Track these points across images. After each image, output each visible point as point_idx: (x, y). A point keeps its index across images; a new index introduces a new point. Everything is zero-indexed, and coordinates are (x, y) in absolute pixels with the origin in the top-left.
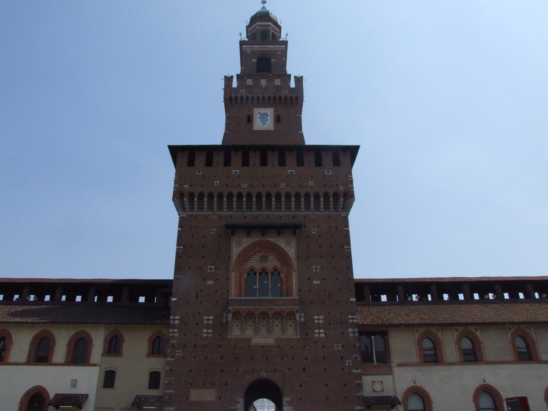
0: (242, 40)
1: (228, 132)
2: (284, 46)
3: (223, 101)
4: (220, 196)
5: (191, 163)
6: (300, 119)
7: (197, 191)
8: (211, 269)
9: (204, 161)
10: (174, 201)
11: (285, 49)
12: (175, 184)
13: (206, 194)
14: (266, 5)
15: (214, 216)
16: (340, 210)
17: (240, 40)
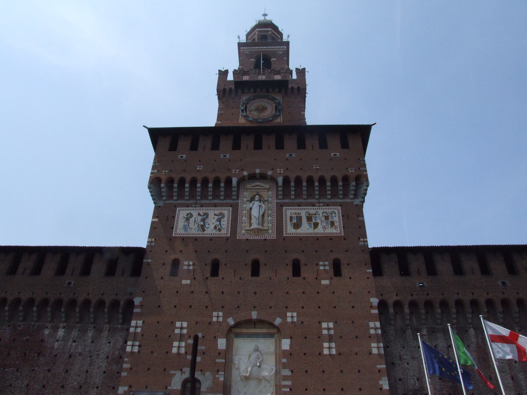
0: (240, 42)
1: (220, 122)
2: (285, 47)
3: (217, 94)
4: (205, 181)
7: (176, 177)
8: (189, 265)
10: (149, 188)
11: (286, 49)
12: (153, 169)
13: (188, 178)
14: (266, 18)
15: (196, 204)
16: (352, 196)
17: (238, 42)
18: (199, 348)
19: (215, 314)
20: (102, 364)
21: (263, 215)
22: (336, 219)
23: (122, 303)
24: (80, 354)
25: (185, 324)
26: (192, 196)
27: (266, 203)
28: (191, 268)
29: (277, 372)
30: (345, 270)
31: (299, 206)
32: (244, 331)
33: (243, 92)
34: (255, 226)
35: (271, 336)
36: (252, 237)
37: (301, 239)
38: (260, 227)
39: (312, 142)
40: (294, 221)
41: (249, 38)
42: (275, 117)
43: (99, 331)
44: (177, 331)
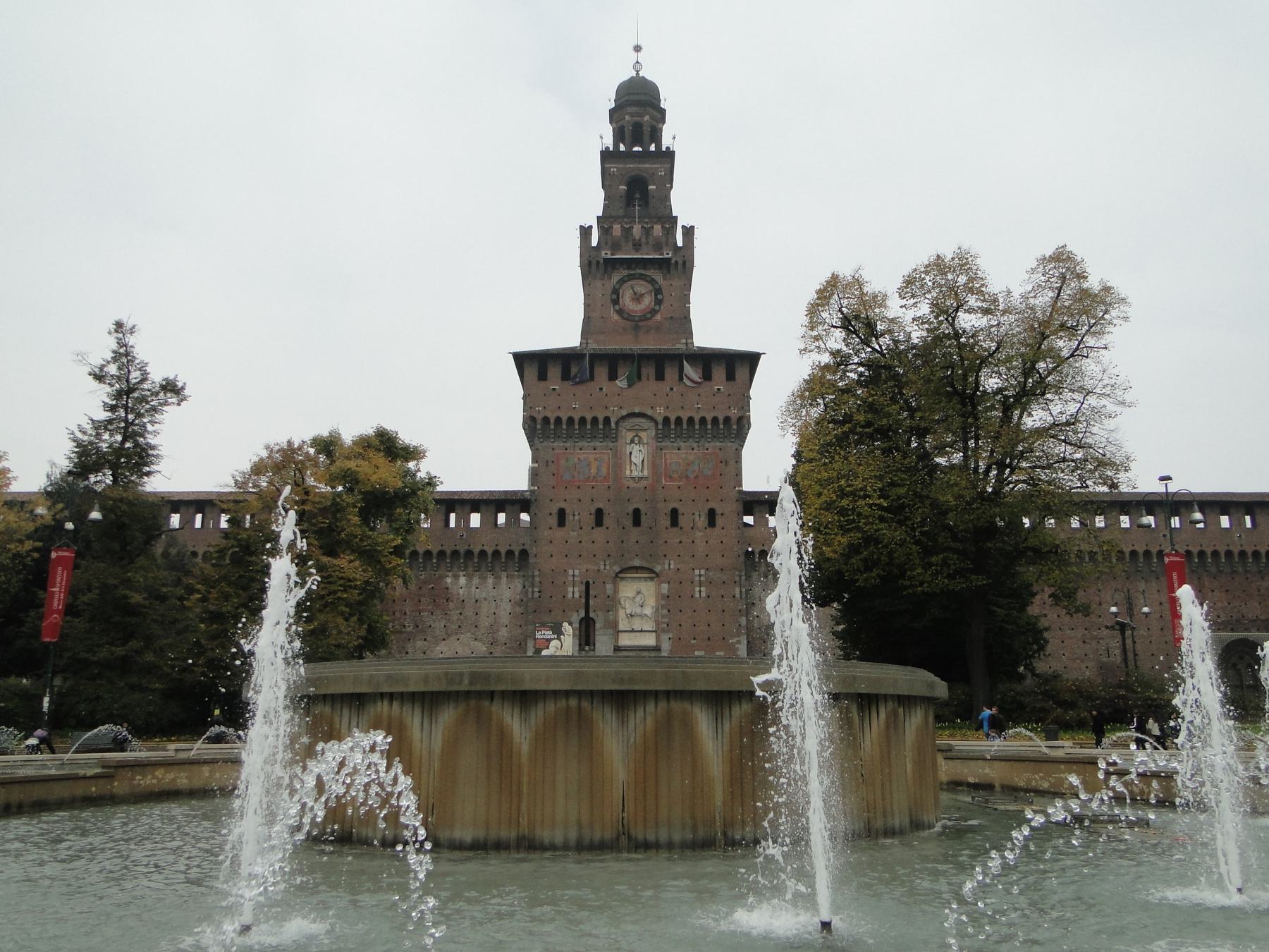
5: (543, 376)
6: (686, 299)
18: (591, 592)
20: (506, 607)
21: (643, 461)
23: (517, 553)
24: (485, 599)
27: (646, 446)
29: (657, 610)
30: (719, 521)
33: (614, 268)
34: (635, 474)
35: (652, 579)
36: (632, 484)
38: (641, 475)
42: (653, 312)
43: (498, 578)
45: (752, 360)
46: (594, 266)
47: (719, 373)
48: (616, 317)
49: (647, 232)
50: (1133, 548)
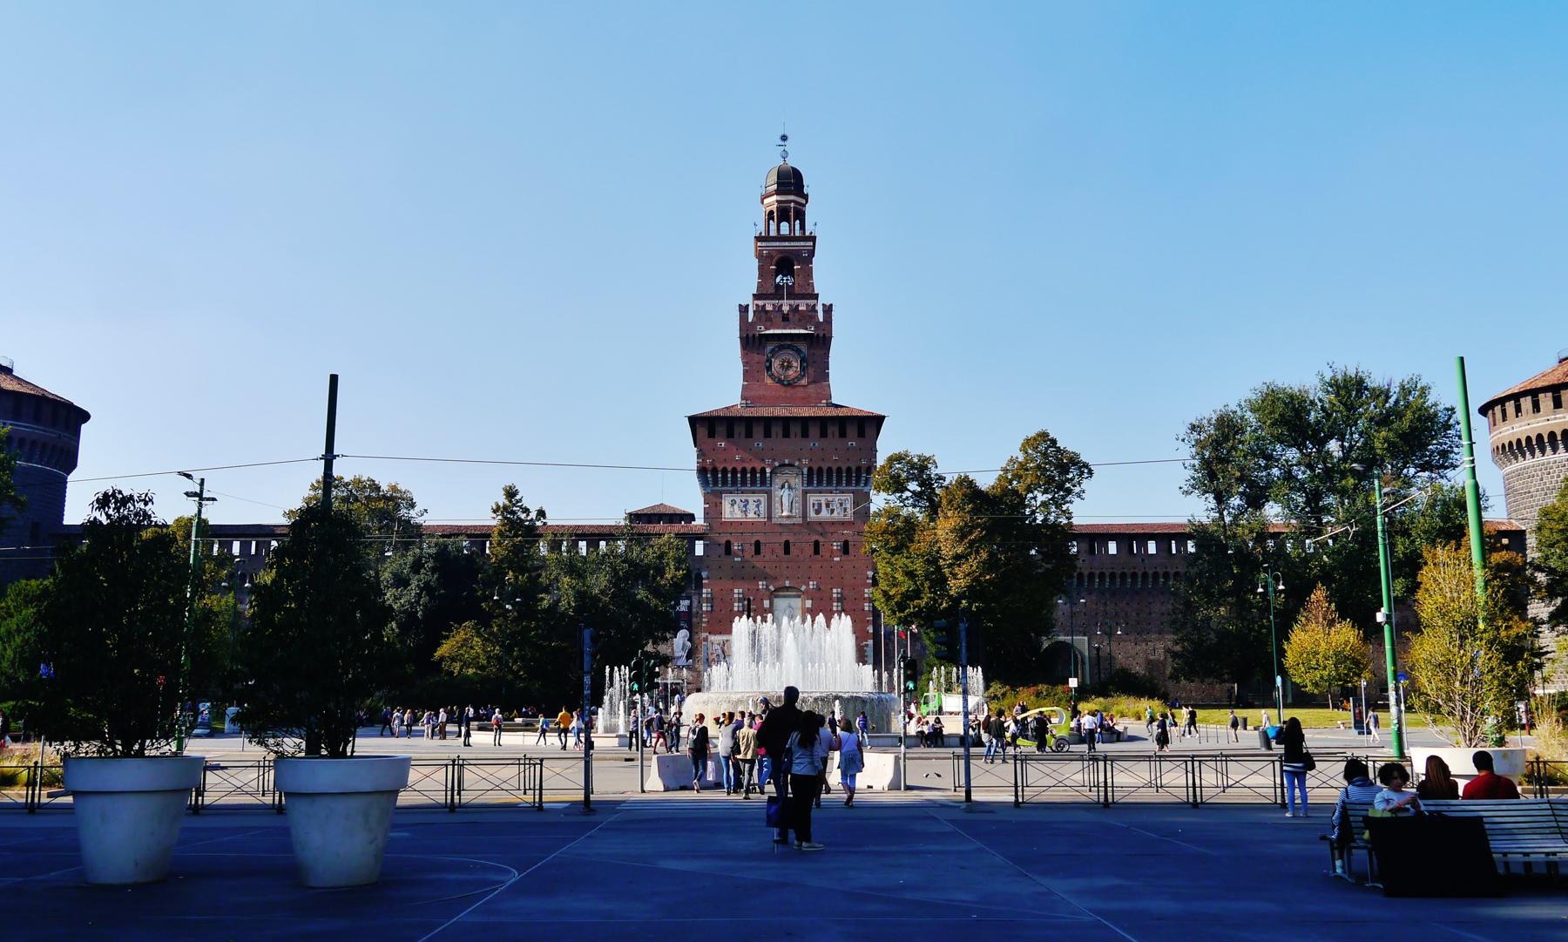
2: (811, 244)
5: (712, 434)
7: (720, 467)
9: (725, 433)
19: (760, 583)
22: (848, 506)
25: (741, 590)
26: (734, 483)
28: (740, 548)
31: (820, 493)
32: (781, 593)
34: (785, 514)
35: (799, 596)
37: (820, 523)
39: (833, 430)
40: (816, 507)
41: (766, 201)
44: (736, 596)
45: (878, 421)
46: (751, 341)
47: (852, 431)
48: (769, 381)
49: (795, 309)
50: (1177, 570)
